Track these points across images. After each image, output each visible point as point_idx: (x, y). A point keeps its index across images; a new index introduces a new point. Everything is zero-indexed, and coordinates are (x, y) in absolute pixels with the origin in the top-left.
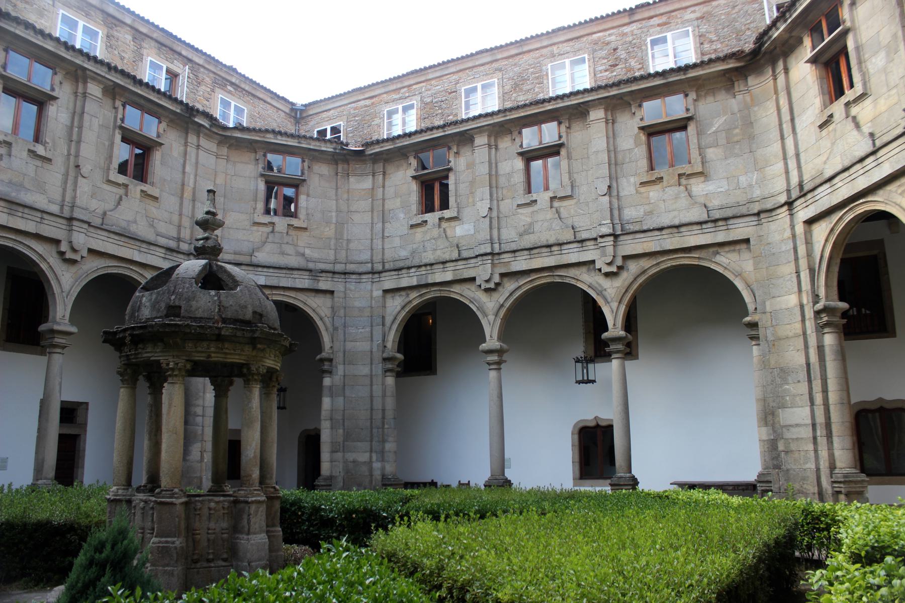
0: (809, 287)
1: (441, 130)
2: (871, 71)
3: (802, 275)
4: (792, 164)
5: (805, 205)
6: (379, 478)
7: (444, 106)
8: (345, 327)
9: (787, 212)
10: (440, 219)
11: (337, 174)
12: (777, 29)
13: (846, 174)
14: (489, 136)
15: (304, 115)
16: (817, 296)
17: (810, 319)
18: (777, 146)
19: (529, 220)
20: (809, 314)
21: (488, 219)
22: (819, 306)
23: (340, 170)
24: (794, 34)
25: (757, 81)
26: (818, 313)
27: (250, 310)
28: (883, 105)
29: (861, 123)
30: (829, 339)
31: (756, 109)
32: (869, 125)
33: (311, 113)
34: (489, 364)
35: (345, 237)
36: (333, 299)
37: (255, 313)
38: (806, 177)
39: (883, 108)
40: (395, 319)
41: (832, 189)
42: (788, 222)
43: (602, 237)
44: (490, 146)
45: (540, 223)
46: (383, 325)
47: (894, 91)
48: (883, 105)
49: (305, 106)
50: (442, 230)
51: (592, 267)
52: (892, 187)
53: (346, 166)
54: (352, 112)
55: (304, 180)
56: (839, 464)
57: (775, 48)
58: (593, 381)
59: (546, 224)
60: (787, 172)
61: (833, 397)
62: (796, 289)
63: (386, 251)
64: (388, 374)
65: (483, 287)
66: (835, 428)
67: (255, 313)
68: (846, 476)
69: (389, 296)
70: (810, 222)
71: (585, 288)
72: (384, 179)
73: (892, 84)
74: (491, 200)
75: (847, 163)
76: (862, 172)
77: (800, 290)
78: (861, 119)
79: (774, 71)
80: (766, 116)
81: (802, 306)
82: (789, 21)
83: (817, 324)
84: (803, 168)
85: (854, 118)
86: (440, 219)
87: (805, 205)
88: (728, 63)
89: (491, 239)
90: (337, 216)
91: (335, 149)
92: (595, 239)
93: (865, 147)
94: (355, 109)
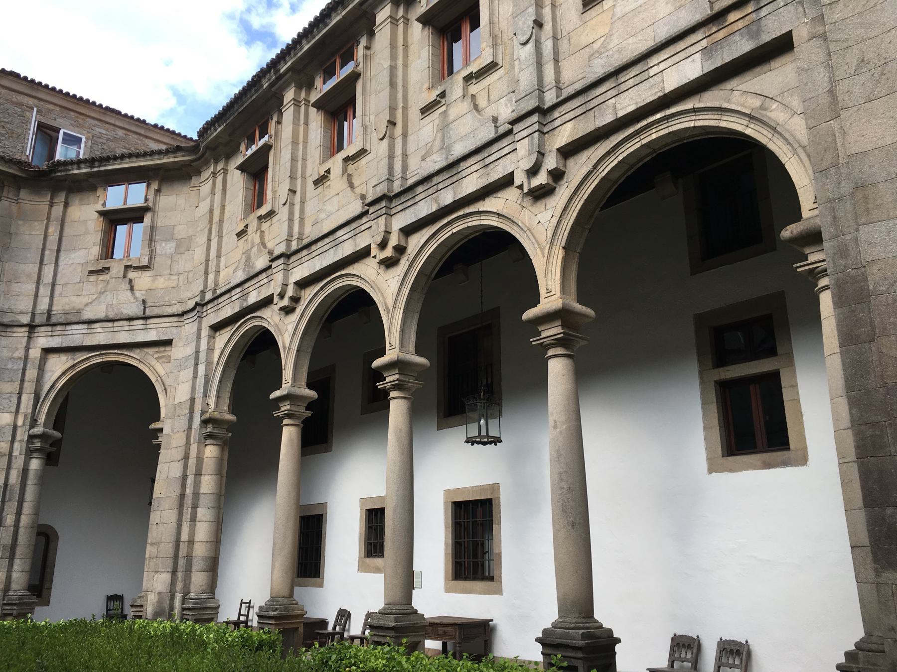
0: (30, 411)
2: (158, 251)
3: (24, 398)
4: (44, 291)
5: (50, 334)
9: (27, 334)
12: (79, 168)
13: (110, 324)
16: (36, 421)
17: (21, 441)
18: (33, 268)
20: (22, 435)
22: (38, 430)
24: (91, 180)
25: (31, 197)
26: (31, 437)
28: (161, 282)
29: (136, 288)
30: (35, 464)
31: (20, 222)
32: (144, 292)
38: (56, 309)
39: (161, 286)
41: (89, 331)
42: (25, 345)
47: (175, 277)
48: (161, 282)
52: (150, 351)
56: (14, 586)
57: (66, 180)
60: (36, 296)
61: (25, 520)
62: (14, 409)
66: (19, 551)
68: (21, 598)
70: (47, 351)
73: (175, 271)
75: (111, 315)
76: (127, 328)
77: (17, 411)
78: (137, 284)
79: (52, 198)
80: (31, 234)
81: (15, 427)
82: (96, 169)
83: (28, 448)
84: (55, 299)
85: (131, 281)
87: (50, 334)
88: (9, 167)
93: (134, 309)
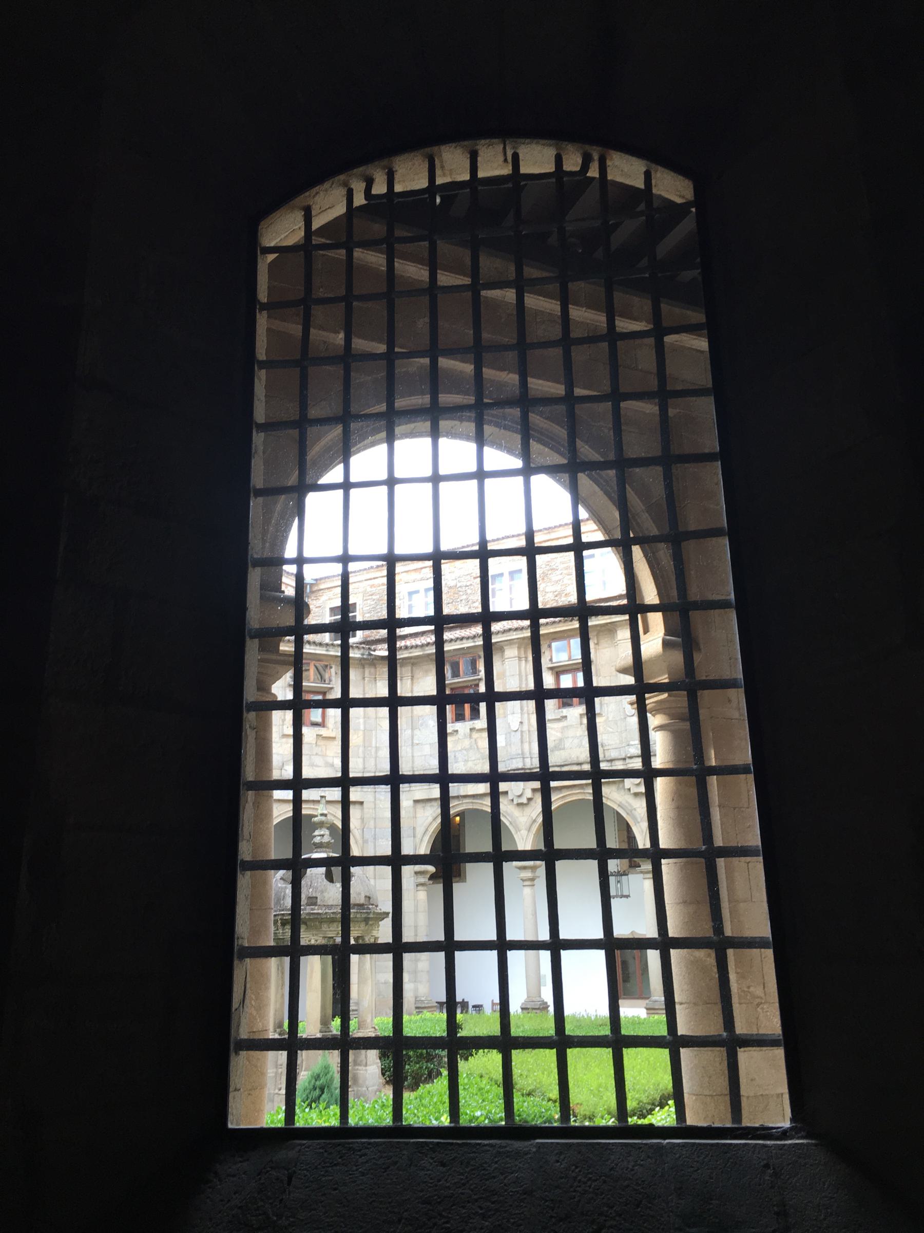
1: (470, 640)
6: (412, 1000)
7: (469, 591)
8: (375, 839)
10: (471, 729)
11: (364, 678)
14: (519, 648)
15: (315, 588)
19: (559, 735)
21: (519, 733)
23: (367, 674)
27: (363, 896)
33: (322, 587)
34: (523, 880)
35: (374, 744)
36: (362, 809)
37: (366, 897)
40: (427, 830)
43: (631, 758)
44: (520, 658)
45: (570, 740)
46: (414, 837)
49: (316, 580)
50: (473, 740)
51: (621, 786)
53: (373, 670)
54: (369, 589)
55: (332, 688)
58: (627, 896)
59: (576, 741)
63: (416, 759)
64: (419, 888)
65: (515, 802)
67: (366, 897)
69: (419, 806)
71: (616, 807)
72: (412, 684)
74: (522, 714)
86: (471, 729)
89: (523, 753)
90: (365, 722)
91: (363, 654)
92: (624, 759)
94: (372, 586)
